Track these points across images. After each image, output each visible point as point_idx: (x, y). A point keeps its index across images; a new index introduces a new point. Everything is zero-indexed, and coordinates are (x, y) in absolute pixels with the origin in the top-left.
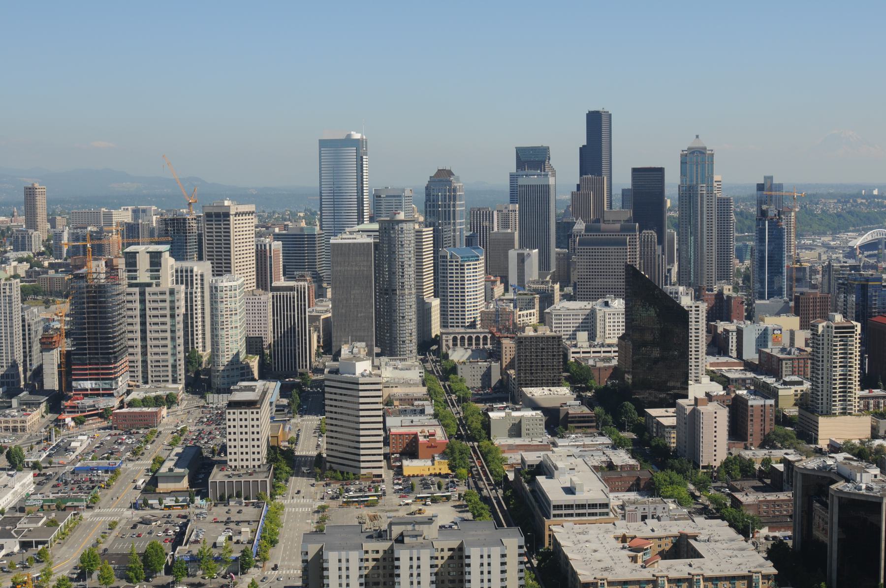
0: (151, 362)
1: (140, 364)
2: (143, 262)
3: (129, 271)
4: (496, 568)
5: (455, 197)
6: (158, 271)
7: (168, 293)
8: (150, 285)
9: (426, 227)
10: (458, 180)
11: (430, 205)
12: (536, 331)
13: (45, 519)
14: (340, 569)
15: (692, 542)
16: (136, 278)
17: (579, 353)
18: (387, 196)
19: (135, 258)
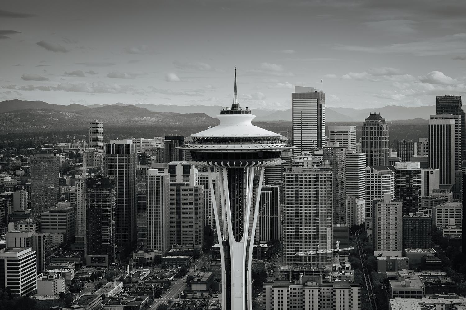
0: (183, 231)
1: (176, 233)
2: (179, 170)
3: (171, 176)
4: (346, 296)
5: (381, 132)
6: (188, 176)
7: (194, 190)
8: (183, 185)
9: (362, 153)
10: (384, 121)
11: (364, 138)
12: (415, 214)
13: (135, 298)
14: (279, 295)
15: (457, 306)
16: (175, 181)
17: (448, 232)
18: (339, 132)
19: (175, 168)
